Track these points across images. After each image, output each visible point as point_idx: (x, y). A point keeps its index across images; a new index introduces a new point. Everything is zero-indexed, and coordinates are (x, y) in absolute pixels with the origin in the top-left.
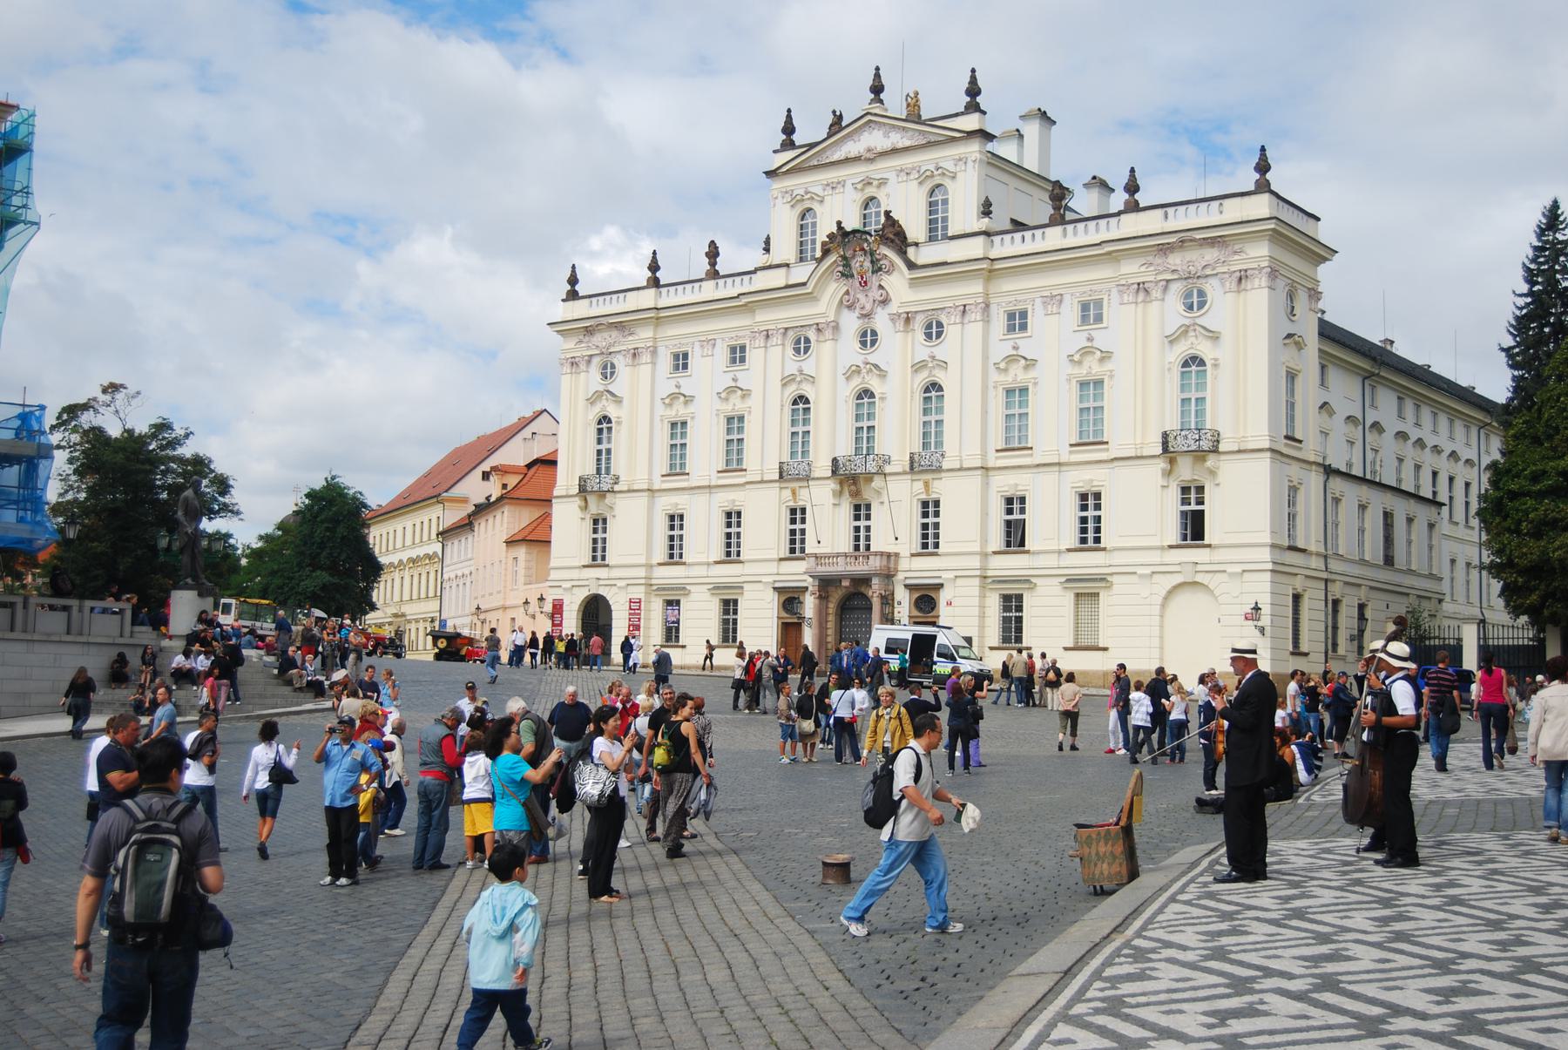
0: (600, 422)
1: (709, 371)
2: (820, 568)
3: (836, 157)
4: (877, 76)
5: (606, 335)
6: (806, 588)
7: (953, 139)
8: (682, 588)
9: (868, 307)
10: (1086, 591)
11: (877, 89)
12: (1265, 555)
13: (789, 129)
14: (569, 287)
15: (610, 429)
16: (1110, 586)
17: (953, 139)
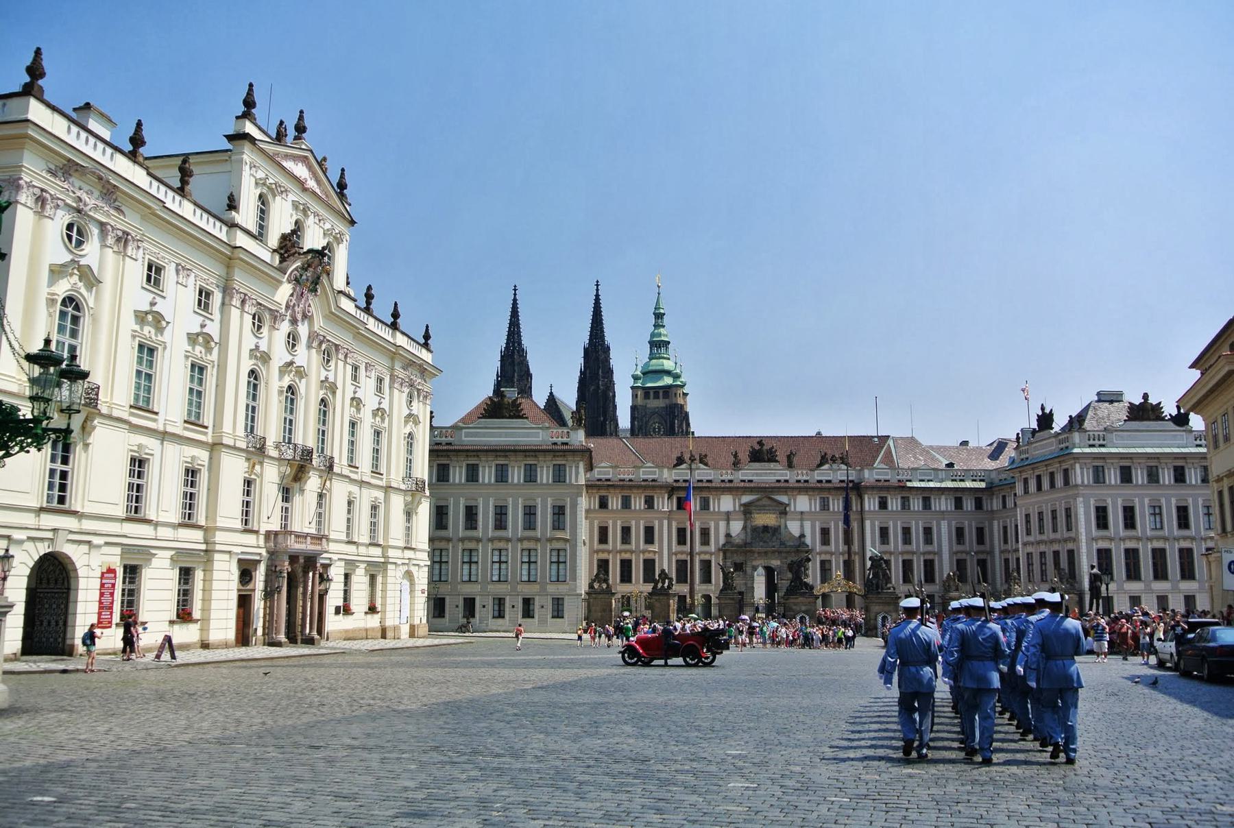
0: (64, 303)
1: (178, 301)
2: (297, 546)
3: (285, 164)
4: (301, 118)
5: (86, 187)
6: (259, 561)
7: (344, 217)
8: (146, 553)
9: (299, 317)
10: (375, 572)
11: (300, 129)
12: (425, 556)
13: (249, 103)
14: (27, 79)
15: (75, 320)
16: (386, 570)
17: (344, 217)
